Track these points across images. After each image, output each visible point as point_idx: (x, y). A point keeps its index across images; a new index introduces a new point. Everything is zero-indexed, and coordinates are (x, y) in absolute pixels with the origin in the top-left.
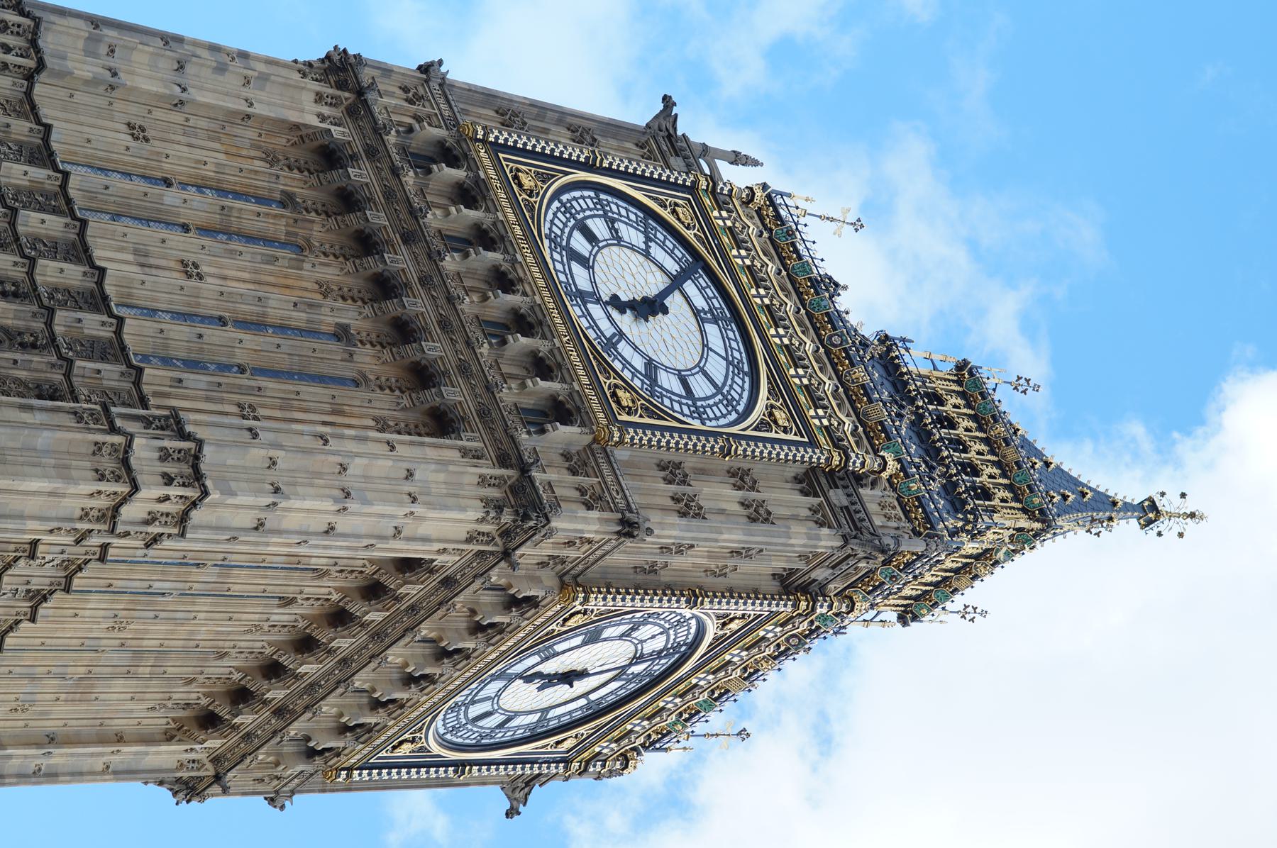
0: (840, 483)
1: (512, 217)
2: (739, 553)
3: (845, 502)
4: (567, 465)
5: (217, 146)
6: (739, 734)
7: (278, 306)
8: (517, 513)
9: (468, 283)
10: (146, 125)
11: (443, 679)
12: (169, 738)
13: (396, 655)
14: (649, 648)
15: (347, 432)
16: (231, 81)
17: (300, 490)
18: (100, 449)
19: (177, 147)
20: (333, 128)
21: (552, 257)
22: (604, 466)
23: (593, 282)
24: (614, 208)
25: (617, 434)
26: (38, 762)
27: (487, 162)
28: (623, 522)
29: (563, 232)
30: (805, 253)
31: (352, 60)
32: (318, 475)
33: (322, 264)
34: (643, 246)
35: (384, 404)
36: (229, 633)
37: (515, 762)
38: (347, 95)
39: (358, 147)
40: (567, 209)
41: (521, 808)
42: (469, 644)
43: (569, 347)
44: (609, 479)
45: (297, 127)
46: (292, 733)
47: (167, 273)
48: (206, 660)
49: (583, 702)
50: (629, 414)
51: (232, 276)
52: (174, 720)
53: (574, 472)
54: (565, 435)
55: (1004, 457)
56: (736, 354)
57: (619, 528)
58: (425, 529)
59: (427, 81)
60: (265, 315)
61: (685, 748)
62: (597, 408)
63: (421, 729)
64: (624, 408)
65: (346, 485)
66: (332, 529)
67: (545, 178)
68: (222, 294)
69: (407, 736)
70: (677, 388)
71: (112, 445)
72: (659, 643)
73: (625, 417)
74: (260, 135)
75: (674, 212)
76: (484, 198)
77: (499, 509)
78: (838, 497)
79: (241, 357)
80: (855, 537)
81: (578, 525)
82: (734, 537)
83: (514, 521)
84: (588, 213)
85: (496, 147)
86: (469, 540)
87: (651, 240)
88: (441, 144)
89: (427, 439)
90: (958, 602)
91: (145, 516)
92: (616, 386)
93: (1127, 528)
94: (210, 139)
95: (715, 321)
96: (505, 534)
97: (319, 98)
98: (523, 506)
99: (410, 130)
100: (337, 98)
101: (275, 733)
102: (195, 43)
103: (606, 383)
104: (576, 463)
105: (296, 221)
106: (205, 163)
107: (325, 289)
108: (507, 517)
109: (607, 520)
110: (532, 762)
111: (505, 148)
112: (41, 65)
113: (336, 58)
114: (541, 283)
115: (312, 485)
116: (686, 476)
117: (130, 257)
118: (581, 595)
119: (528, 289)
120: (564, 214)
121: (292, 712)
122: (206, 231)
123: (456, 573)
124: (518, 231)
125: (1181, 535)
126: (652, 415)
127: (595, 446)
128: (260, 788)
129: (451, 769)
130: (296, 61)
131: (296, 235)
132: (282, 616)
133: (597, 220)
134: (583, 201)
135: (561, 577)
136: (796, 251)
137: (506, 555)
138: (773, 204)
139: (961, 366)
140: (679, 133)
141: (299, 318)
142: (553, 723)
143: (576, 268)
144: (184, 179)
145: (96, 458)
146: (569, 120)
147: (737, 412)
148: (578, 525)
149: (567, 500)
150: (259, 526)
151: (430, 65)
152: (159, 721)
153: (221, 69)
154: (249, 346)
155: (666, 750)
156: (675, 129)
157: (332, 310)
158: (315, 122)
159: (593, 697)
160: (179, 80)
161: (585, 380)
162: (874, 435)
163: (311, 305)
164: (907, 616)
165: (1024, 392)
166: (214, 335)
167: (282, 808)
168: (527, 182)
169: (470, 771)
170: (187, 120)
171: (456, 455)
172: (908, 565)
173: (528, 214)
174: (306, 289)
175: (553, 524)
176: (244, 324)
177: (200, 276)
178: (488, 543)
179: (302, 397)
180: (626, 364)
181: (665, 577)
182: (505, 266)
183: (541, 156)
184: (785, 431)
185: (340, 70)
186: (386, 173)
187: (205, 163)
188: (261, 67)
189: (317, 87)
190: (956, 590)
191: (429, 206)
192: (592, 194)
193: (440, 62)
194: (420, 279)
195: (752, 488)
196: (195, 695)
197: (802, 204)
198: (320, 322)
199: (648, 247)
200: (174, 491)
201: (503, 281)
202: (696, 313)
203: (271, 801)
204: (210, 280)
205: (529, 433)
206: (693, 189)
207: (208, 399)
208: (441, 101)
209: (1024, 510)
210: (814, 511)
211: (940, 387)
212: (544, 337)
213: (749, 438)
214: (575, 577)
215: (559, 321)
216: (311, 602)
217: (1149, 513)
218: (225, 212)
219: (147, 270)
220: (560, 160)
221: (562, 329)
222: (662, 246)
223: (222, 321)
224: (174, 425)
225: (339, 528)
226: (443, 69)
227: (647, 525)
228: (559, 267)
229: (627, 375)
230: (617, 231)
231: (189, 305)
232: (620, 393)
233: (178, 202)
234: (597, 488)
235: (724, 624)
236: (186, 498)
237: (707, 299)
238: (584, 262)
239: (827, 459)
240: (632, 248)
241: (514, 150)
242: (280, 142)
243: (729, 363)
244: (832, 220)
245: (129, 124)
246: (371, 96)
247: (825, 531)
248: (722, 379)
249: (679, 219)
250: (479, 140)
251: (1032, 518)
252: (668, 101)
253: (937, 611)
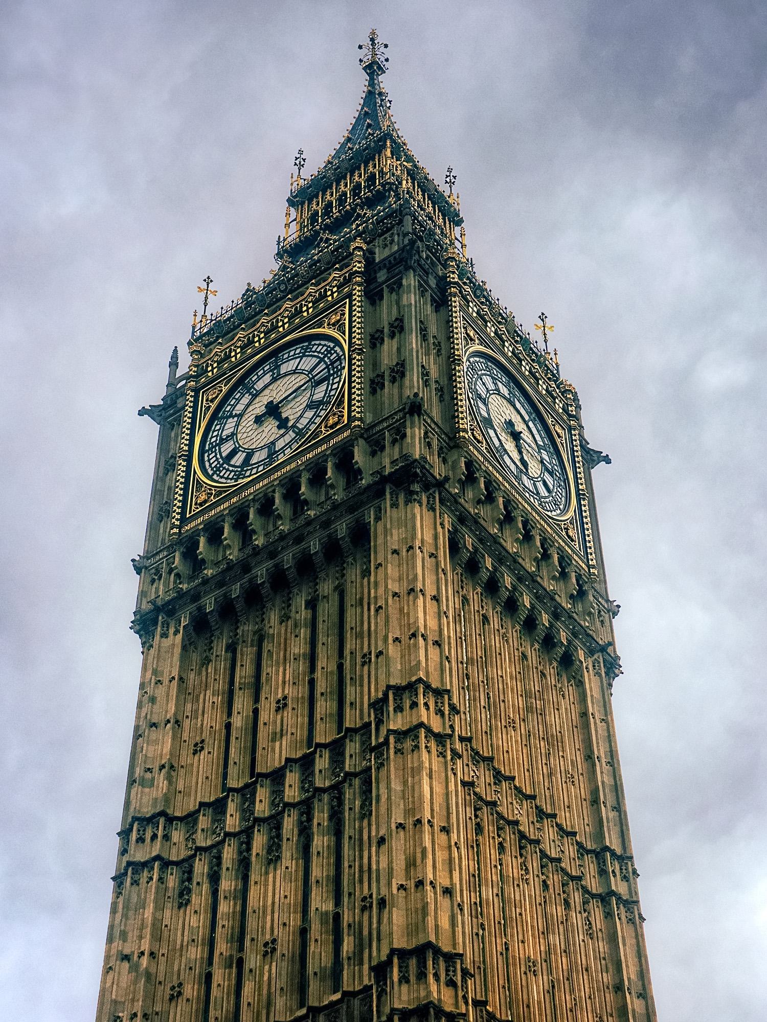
0: (373, 276)
1: (226, 505)
2: (424, 336)
3: (385, 270)
4: (379, 453)
5: (202, 696)
6: (543, 320)
7: (298, 647)
8: (413, 482)
9: (271, 528)
10: (194, 743)
12: (580, 684)
13: (512, 547)
14: (491, 386)
15: (372, 595)
16: (160, 692)
17: (412, 621)
18: (399, 750)
19: (205, 722)
20: (182, 625)
21: (249, 476)
22: (378, 429)
23: (262, 448)
24: (214, 439)
25: (357, 423)
26: (604, 764)
27: (193, 524)
28: (412, 414)
29: (232, 471)
30: (229, 314)
31: (138, 617)
32: (401, 610)
33: (269, 622)
34: (236, 419)
35: (353, 573)
36: (509, 654)
37: (574, 462)
38: (160, 618)
39: (193, 607)
40: (217, 470)
43: (304, 459)
44: (385, 425)
45: (184, 648)
46: (569, 606)
47: (285, 719)
48: (528, 666)
49: (531, 424)
50: (343, 416)
51: (283, 679)
52: (568, 682)
53: (383, 448)
54: (359, 456)
55: (347, 169)
56: (298, 351)
58: (428, 538)
59: (146, 568)
60: (304, 655)
61: (556, 354)
62: (340, 438)
63: (559, 525)
64: (339, 420)
65: (406, 592)
66: (434, 597)
67: (199, 484)
68: (294, 683)
69: (564, 533)
70: (323, 387)
71: (395, 742)
72: (488, 380)
73: (346, 418)
74: (192, 670)
75: (212, 401)
76: (218, 523)
77: (412, 493)
78: (382, 276)
79: (333, 667)
80: (406, 262)
81: (416, 442)
82: (414, 341)
83: (418, 483)
84: (218, 456)
85: (184, 520)
86: (434, 510)
87: (231, 413)
88: (184, 556)
89: (372, 544)
90: (444, 188)
91: (439, 716)
92: (326, 427)
93: (385, 82)
94: (198, 701)
95: (278, 367)
96: (426, 487)
97: (164, 635)
98: (408, 479)
99: (178, 576)
100: (163, 624)
101: (571, 617)
102: (138, 717)
103: (324, 433)
104: (376, 447)
105: (244, 642)
106: (214, 703)
107: (285, 618)
108: (416, 487)
109: (412, 423)
110: (573, 451)
111: (183, 514)
112: (162, 813)
113: (137, 627)
114: (266, 481)
115: (408, 614)
116: (378, 376)
117: (278, 744)
118: (461, 434)
119: (270, 490)
120: (221, 472)
122: (257, 700)
123: (455, 515)
124: (235, 500)
125: (386, 46)
126: (342, 402)
127: (365, 436)
128: (607, 623)
129: (582, 503)
130: (143, 653)
131: (252, 640)
132: (495, 622)
133: (222, 450)
134: (211, 460)
135: (452, 448)
136: (229, 319)
138: (200, 337)
140: (162, 403)
141: (304, 632)
143: (254, 460)
144: (225, 717)
145: (405, 751)
146: (161, 475)
147: (334, 347)
148: (416, 442)
149: (401, 450)
150: (437, 643)
151: (134, 566)
152: (571, 691)
153: (153, 700)
154: (325, 662)
156: (160, 406)
157: (297, 612)
158: (179, 637)
159: (527, 418)
160: (163, 725)
161: (324, 447)
162: (341, 257)
163: (296, 626)
164: (456, 220)
165: (304, 160)
166: (321, 686)
167: (619, 606)
168: (203, 497)
169: (583, 490)
170: (187, 717)
171: (380, 525)
172: (422, 226)
173: (223, 494)
174: (286, 630)
175: (417, 457)
176: (312, 669)
177: (285, 698)
178: (434, 498)
179: (353, 625)
180: (311, 422)
181: (444, 381)
182: (257, 505)
183: (186, 490)
184: (344, 314)
185: (146, 624)
186: (207, 587)
187: (214, 703)
188: (149, 674)
189: (157, 638)
190: (436, 190)
191: (225, 558)
192: (206, 455)
193: (133, 560)
194: (271, 559)
195: (382, 332)
196: (551, 671)
197: (198, 319)
198: (305, 619)
199: (236, 415)
200: (421, 701)
201: (266, 507)
202: (274, 380)
203: (615, 614)
204: (286, 692)
205: (361, 479)
206: (196, 391)
207: (362, 686)
208: (158, 558)
209: (380, 153)
210: (392, 290)
211: (306, 214)
212: (300, 476)
213: (350, 338)
214: (450, 439)
215: (288, 468)
216: (484, 604)
217: (373, 69)
218: (242, 686)
219: (284, 732)
220: (187, 478)
221: (293, 465)
222: (234, 406)
223: (312, 683)
224: (379, 706)
225: (434, 593)
226: (138, 558)
227: (412, 397)
228: (254, 471)
229: (318, 420)
230: (228, 437)
231: (303, 703)
232: (331, 422)
233: (240, 717)
234: (392, 432)
235: (471, 340)
236: (424, 692)
237: (265, 374)
238: (249, 455)
239: (359, 286)
240: (237, 425)
241: (184, 507)
242: (195, 657)
243: (304, 356)
244: (206, 298)
245: (194, 754)
246: (159, 603)
247: (404, 282)
248: (314, 359)
249: (216, 397)
250: (180, 531)
251: (384, 146)
252: (142, 412)
253: (451, 201)
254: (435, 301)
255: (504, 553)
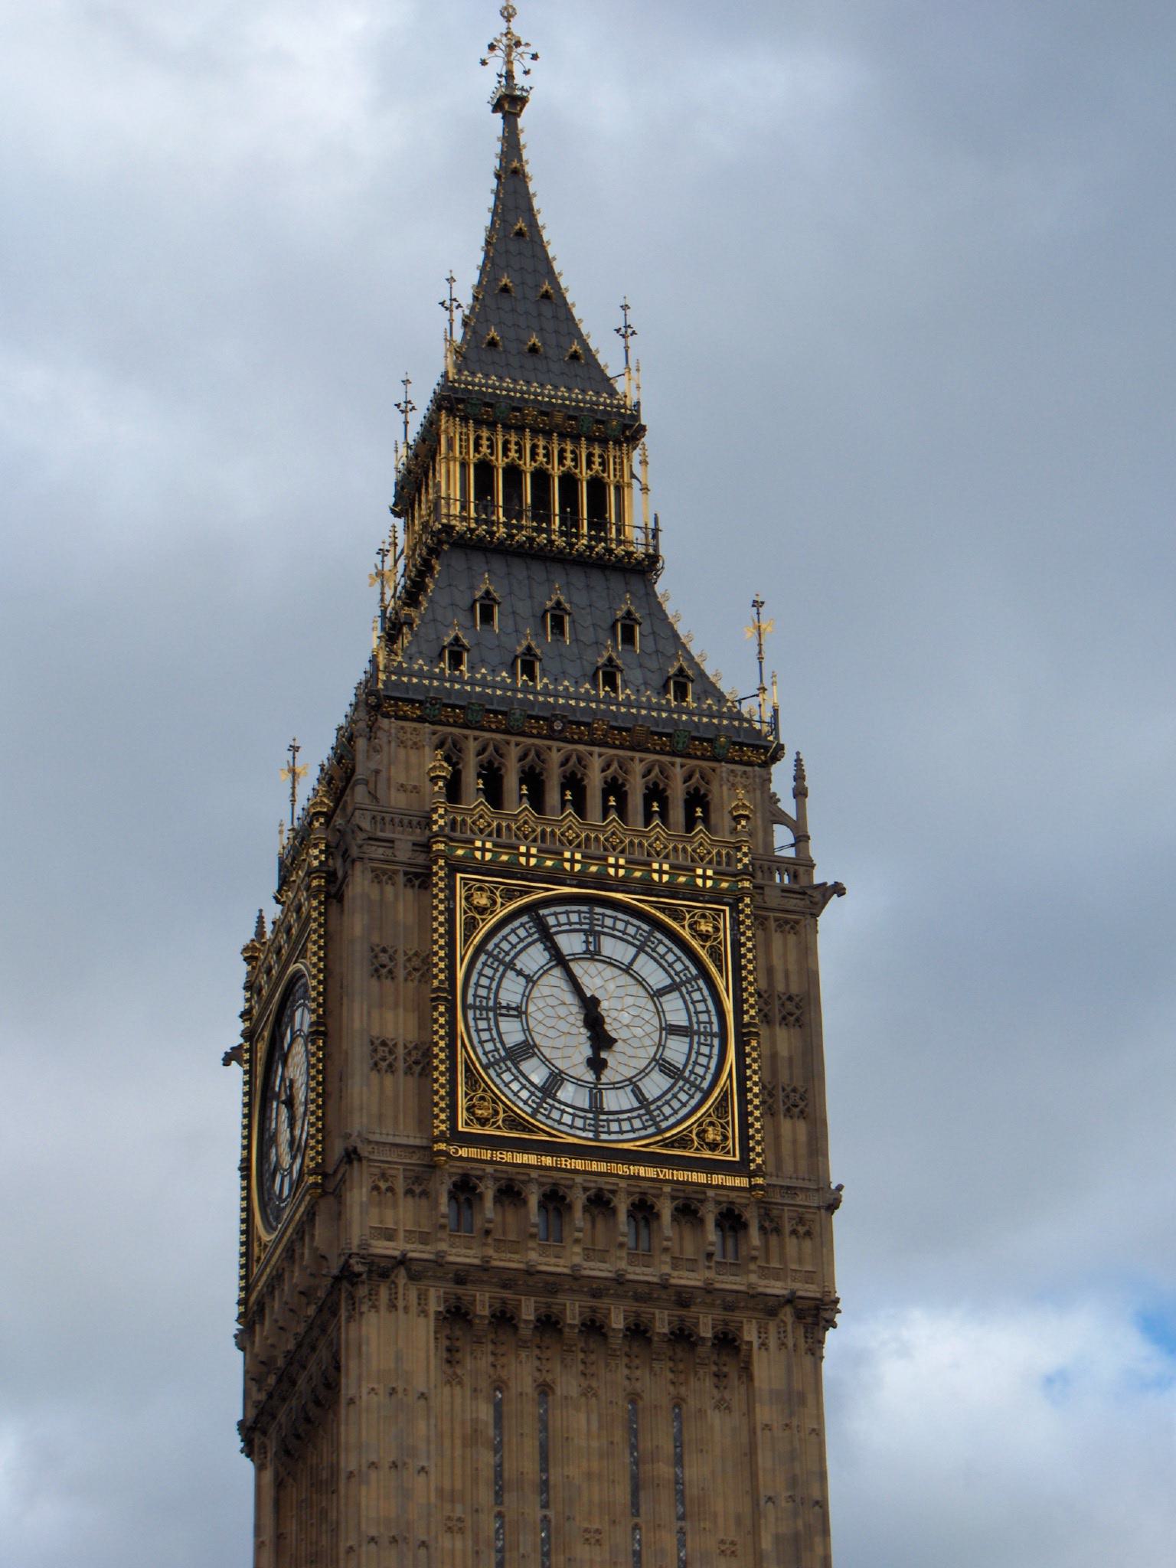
2: (390, 972)
11: (592, 1185)
28: (350, 1162)
41: (830, 883)
42: (533, 1201)
46: (710, 1274)
57: (356, 1164)
83: (363, 1283)
96: (384, 1274)
108: (362, 1291)
121: (679, 1294)
137: (403, 1261)
139: (397, 514)
142: (682, 965)
155: (776, 711)
167: (840, 1188)
203: (833, 1206)
235: (482, 910)
252: (227, 1060)
254: (417, 875)
255: (551, 1279)
